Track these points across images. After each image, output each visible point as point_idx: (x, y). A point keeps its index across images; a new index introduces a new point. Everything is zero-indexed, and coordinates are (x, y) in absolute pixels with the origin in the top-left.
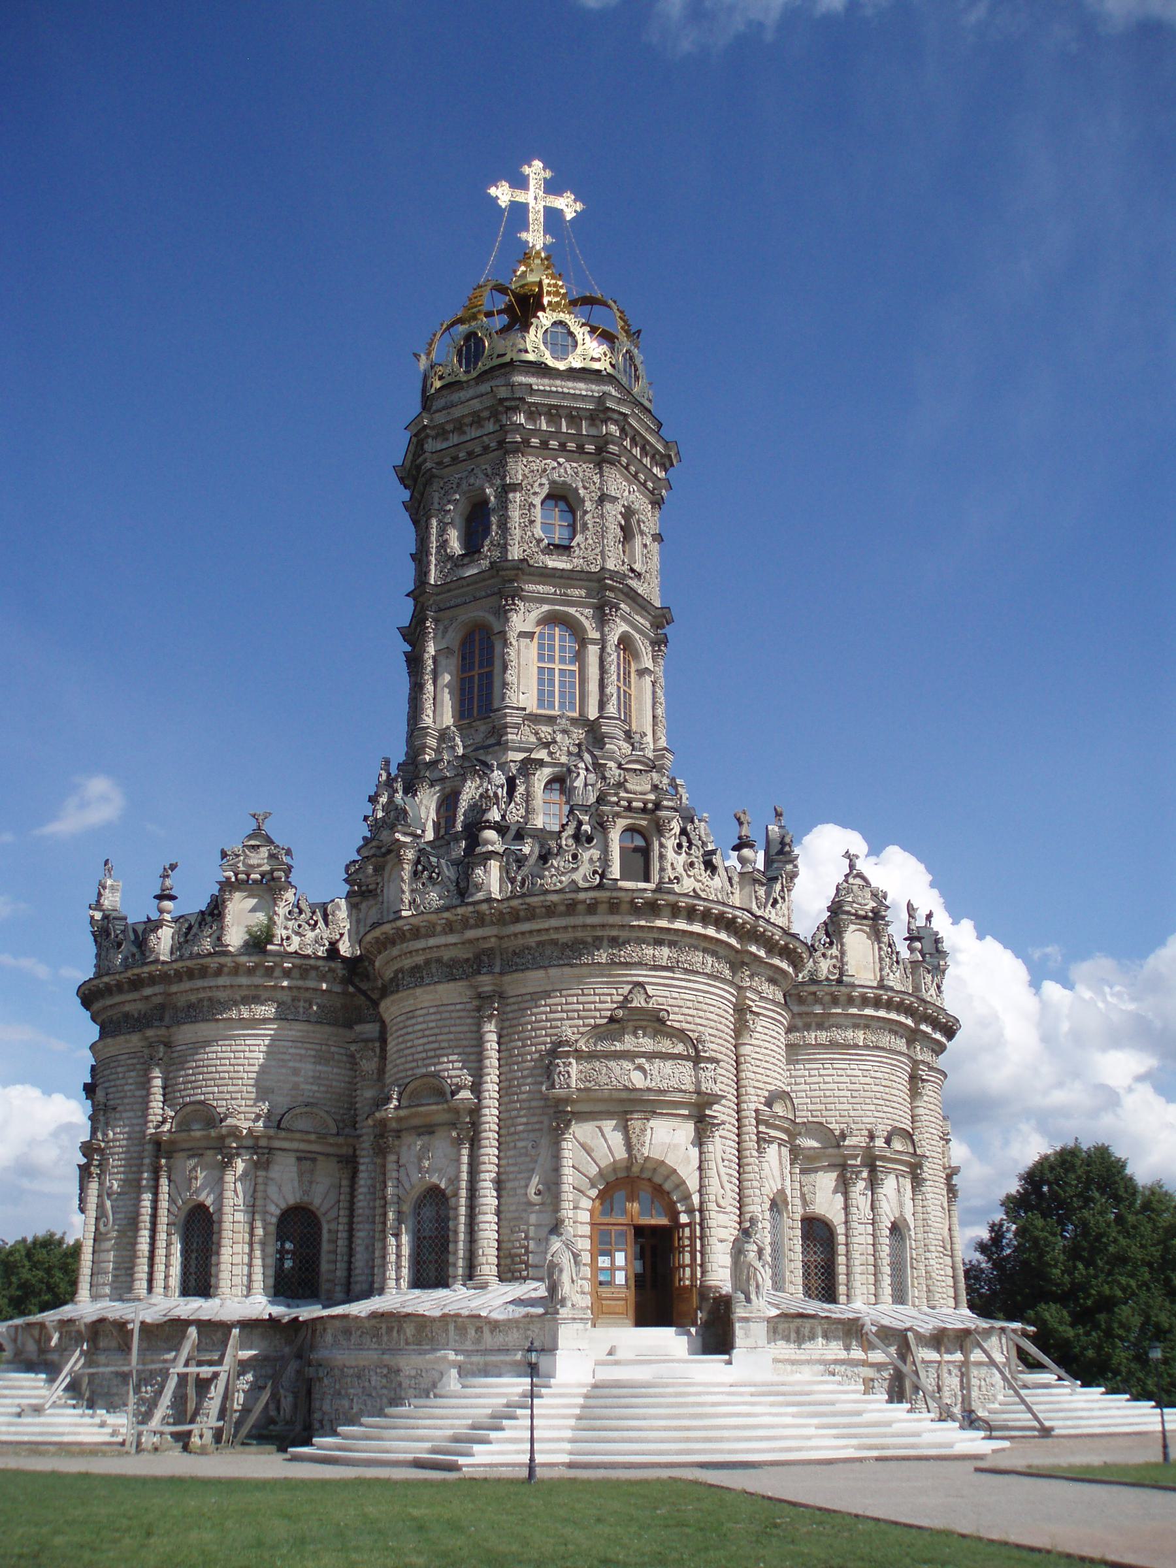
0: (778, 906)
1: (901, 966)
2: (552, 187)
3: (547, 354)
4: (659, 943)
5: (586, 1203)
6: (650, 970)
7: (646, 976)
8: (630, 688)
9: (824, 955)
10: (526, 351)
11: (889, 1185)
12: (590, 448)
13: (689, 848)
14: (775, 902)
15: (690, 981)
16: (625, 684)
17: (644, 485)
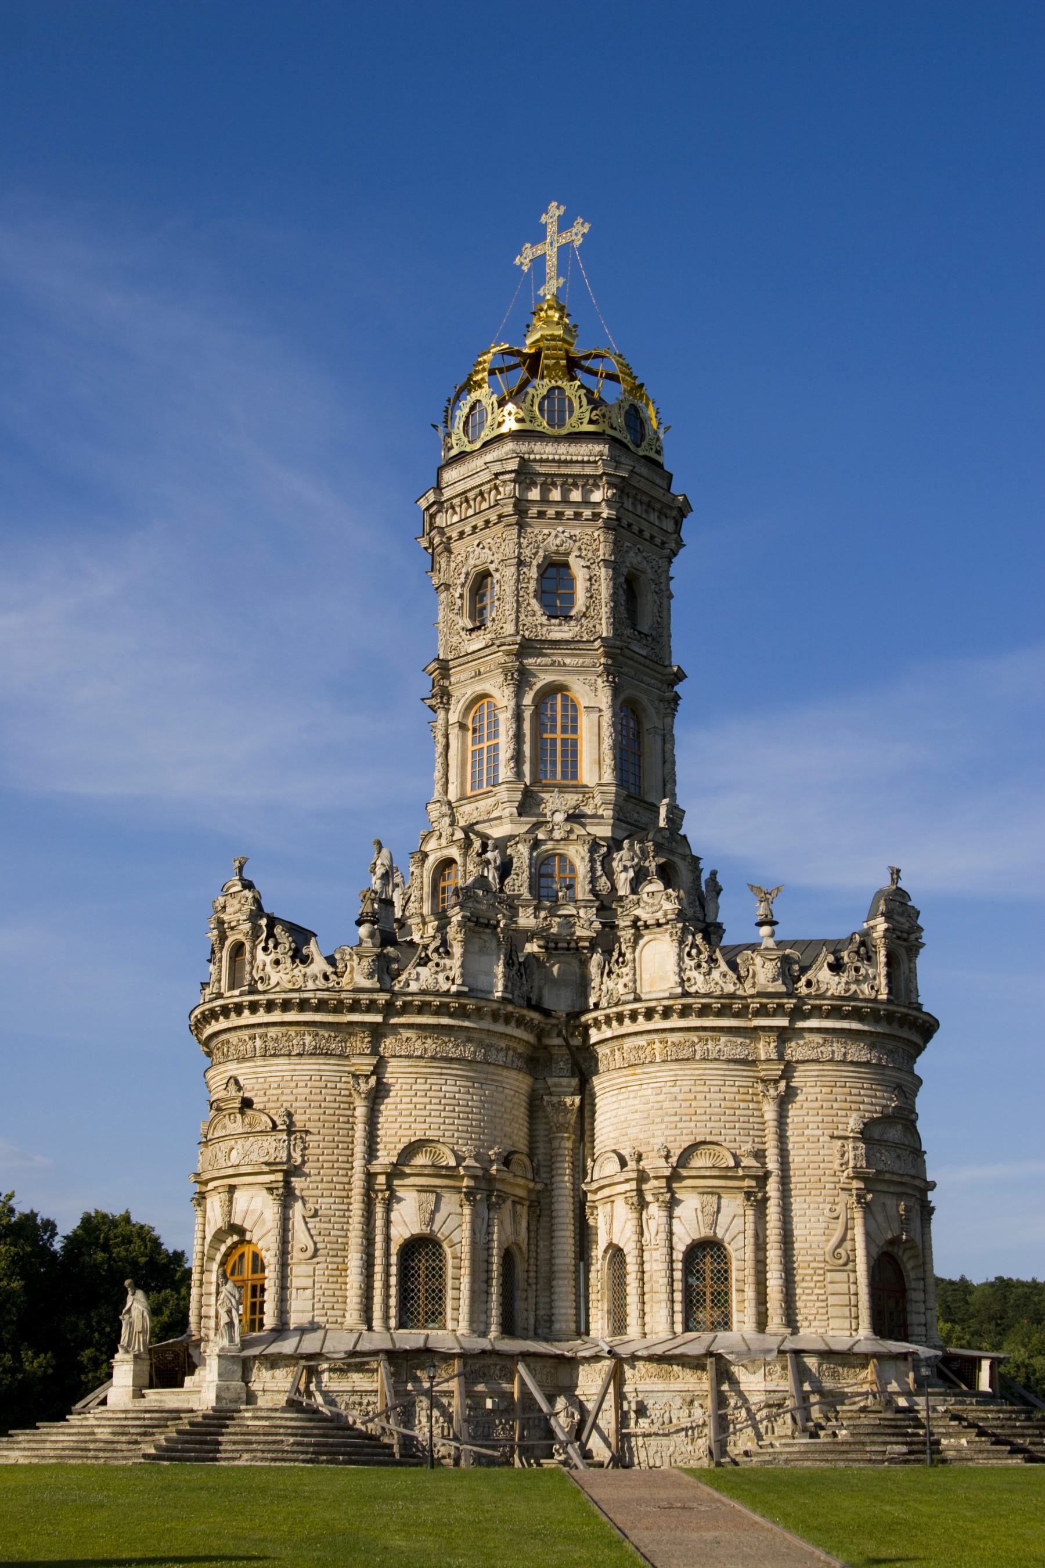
0: (430, 964)
1: (722, 962)
2: (564, 224)
3: (466, 440)
4: (253, 1038)
5: (215, 1266)
6: (239, 1063)
7: (237, 1069)
8: (575, 730)
9: (618, 975)
10: (452, 448)
11: (690, 1204)
12: (494, 518)
13: (275, 947)
14: (424, 962)
15: (272, 1065)
16: (564, 730)
17: (578, 516)
